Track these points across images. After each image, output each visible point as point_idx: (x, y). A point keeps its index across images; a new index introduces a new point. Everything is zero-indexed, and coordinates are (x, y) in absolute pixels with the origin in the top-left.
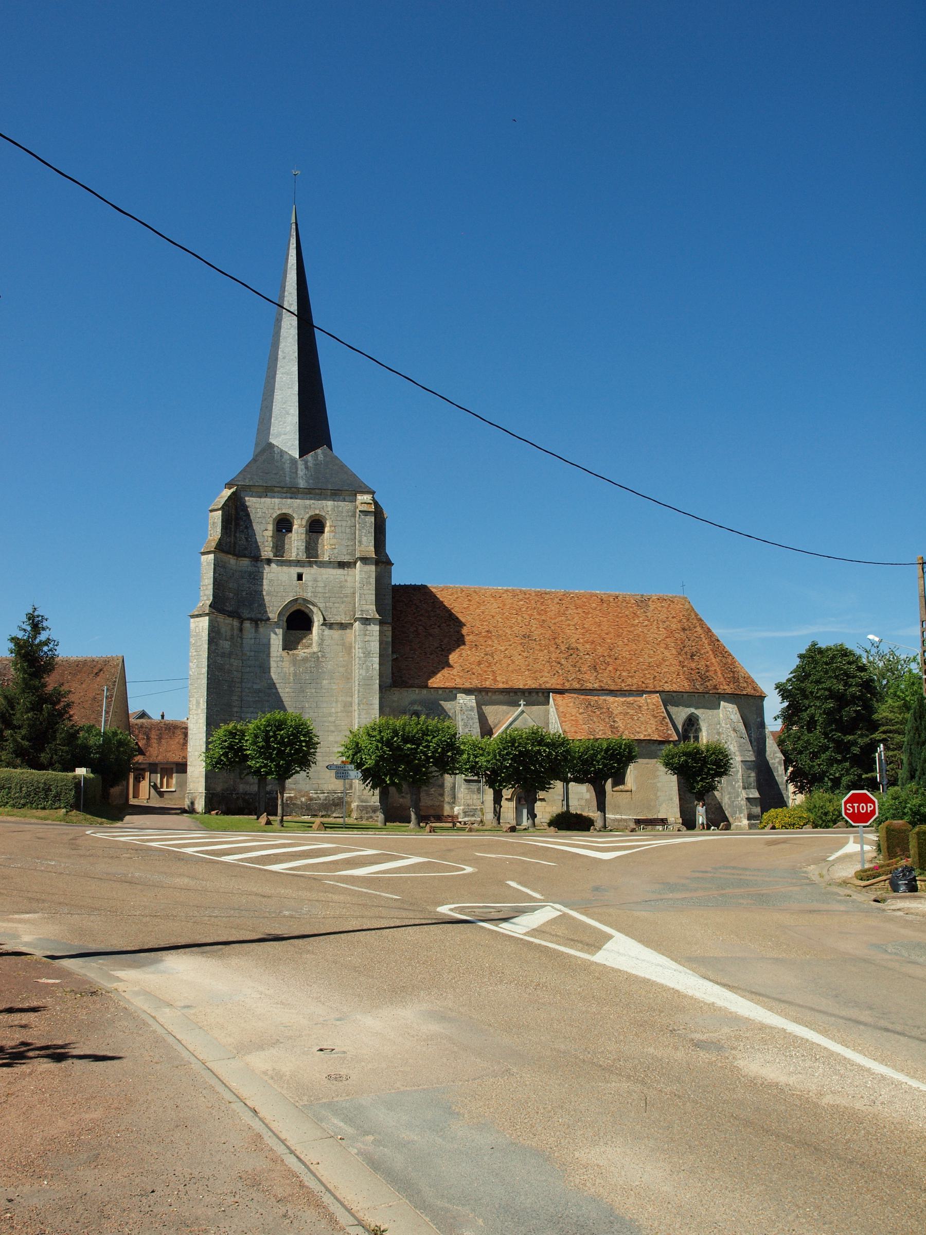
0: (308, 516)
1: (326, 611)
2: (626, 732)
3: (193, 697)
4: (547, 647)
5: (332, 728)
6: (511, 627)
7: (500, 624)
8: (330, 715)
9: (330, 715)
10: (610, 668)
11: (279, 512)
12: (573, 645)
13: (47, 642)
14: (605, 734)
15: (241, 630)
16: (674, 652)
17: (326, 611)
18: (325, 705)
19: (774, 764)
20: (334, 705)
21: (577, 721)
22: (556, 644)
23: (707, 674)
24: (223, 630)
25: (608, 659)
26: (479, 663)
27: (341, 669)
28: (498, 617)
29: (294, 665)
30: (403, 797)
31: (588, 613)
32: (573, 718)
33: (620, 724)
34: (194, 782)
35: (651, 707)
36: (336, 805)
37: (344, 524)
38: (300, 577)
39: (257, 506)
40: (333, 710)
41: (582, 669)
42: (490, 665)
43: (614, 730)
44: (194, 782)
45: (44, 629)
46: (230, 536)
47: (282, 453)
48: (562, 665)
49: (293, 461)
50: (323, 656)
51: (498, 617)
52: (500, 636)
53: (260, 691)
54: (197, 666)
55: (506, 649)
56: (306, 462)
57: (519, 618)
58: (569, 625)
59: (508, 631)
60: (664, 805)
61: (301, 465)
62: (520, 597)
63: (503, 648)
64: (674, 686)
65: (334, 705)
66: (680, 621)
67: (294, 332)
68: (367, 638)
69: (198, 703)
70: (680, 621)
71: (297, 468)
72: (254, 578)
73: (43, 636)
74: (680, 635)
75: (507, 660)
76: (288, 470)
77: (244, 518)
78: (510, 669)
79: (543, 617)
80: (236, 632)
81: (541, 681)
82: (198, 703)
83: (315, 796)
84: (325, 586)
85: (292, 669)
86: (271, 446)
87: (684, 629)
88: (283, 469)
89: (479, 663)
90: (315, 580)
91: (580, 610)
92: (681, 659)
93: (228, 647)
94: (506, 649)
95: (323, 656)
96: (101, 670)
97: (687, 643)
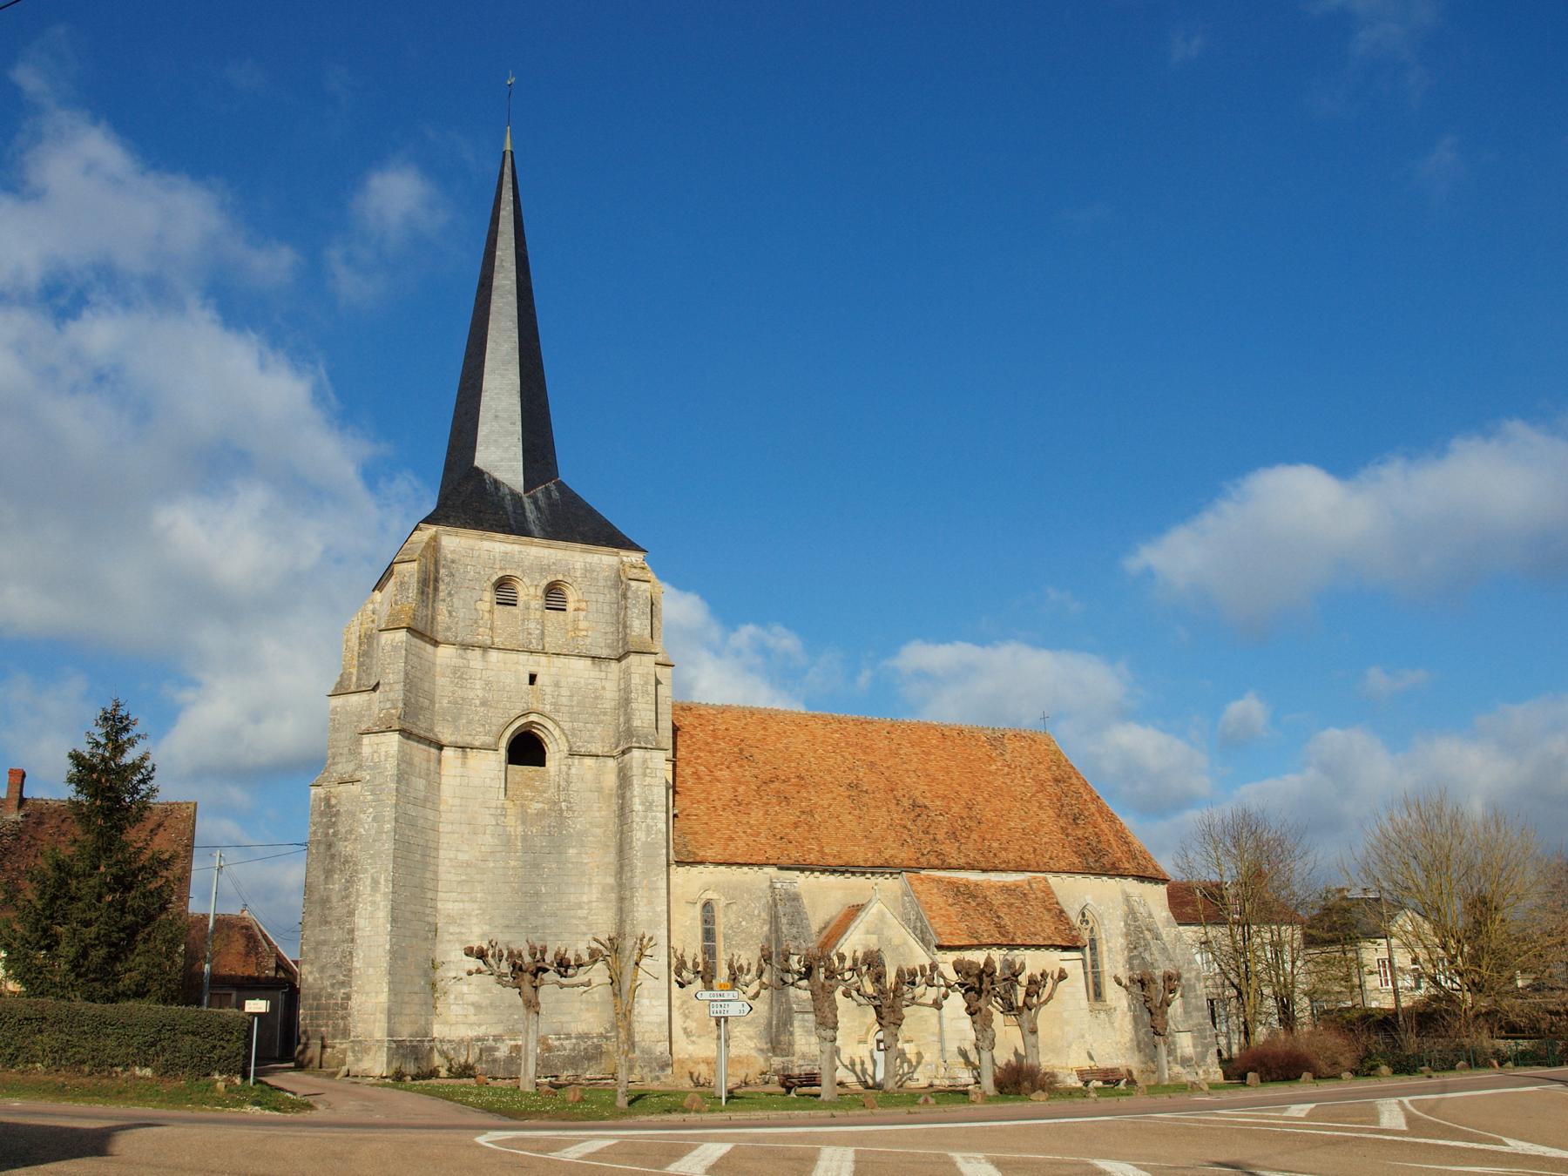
0: (545, 583)
1: (574, 735)
3: (366, 871)
5: (584, 929)
6: (830, 772)
8: (580, 906)
9: (580, 906)
10: (974, 836)
11: (501, 574)
12: (921, 801)
13: (135, 767)
15: (440, 761)
16: (1051, 812)
17: (574, 735)
19: (1188, 979)
20: (586, 889)
21: (949, 917)
24: (416, 760)
27: (598, 831)
28: (809, 755)
29: (524, 823)
31: (927, 754)
33: (1007, 921)
34: (365, 1022)
36: (590, 1059)
37: (601, 598)
38: (533, 679)
39: (468, 561)
40: (585, 898)
44: (365, 1022)
45: (131, 742)
47: (496, 481)
49: (513, 494)
50: (568, 809)
51: (809, 755)
52: (817, 784)
53: (468, 865)
54: (374, 819)
56: (535, 501)
61: (526, 500)
65: (586, 889)
67: (513, 299)
69: (375, 882)
70: (1049, 769)
71: (523, 508)
73: (130, 757)
75: (834, 821)
76: (510, 508)
77: (447, 579)
78: (841, 836)
79: (871, 758)
80: (433, 765)
81: (887, 854)
82: (375, 882)
84: (572, 696)
85: (520, 829)
86: (479, 473)
87: (1057, 781)
88: (504, 508)
89: (796, 825)
90: (557, 685)
91: (917, 750)
92: (1061, 823)
96: (160, 825)
97: (1066, 801)
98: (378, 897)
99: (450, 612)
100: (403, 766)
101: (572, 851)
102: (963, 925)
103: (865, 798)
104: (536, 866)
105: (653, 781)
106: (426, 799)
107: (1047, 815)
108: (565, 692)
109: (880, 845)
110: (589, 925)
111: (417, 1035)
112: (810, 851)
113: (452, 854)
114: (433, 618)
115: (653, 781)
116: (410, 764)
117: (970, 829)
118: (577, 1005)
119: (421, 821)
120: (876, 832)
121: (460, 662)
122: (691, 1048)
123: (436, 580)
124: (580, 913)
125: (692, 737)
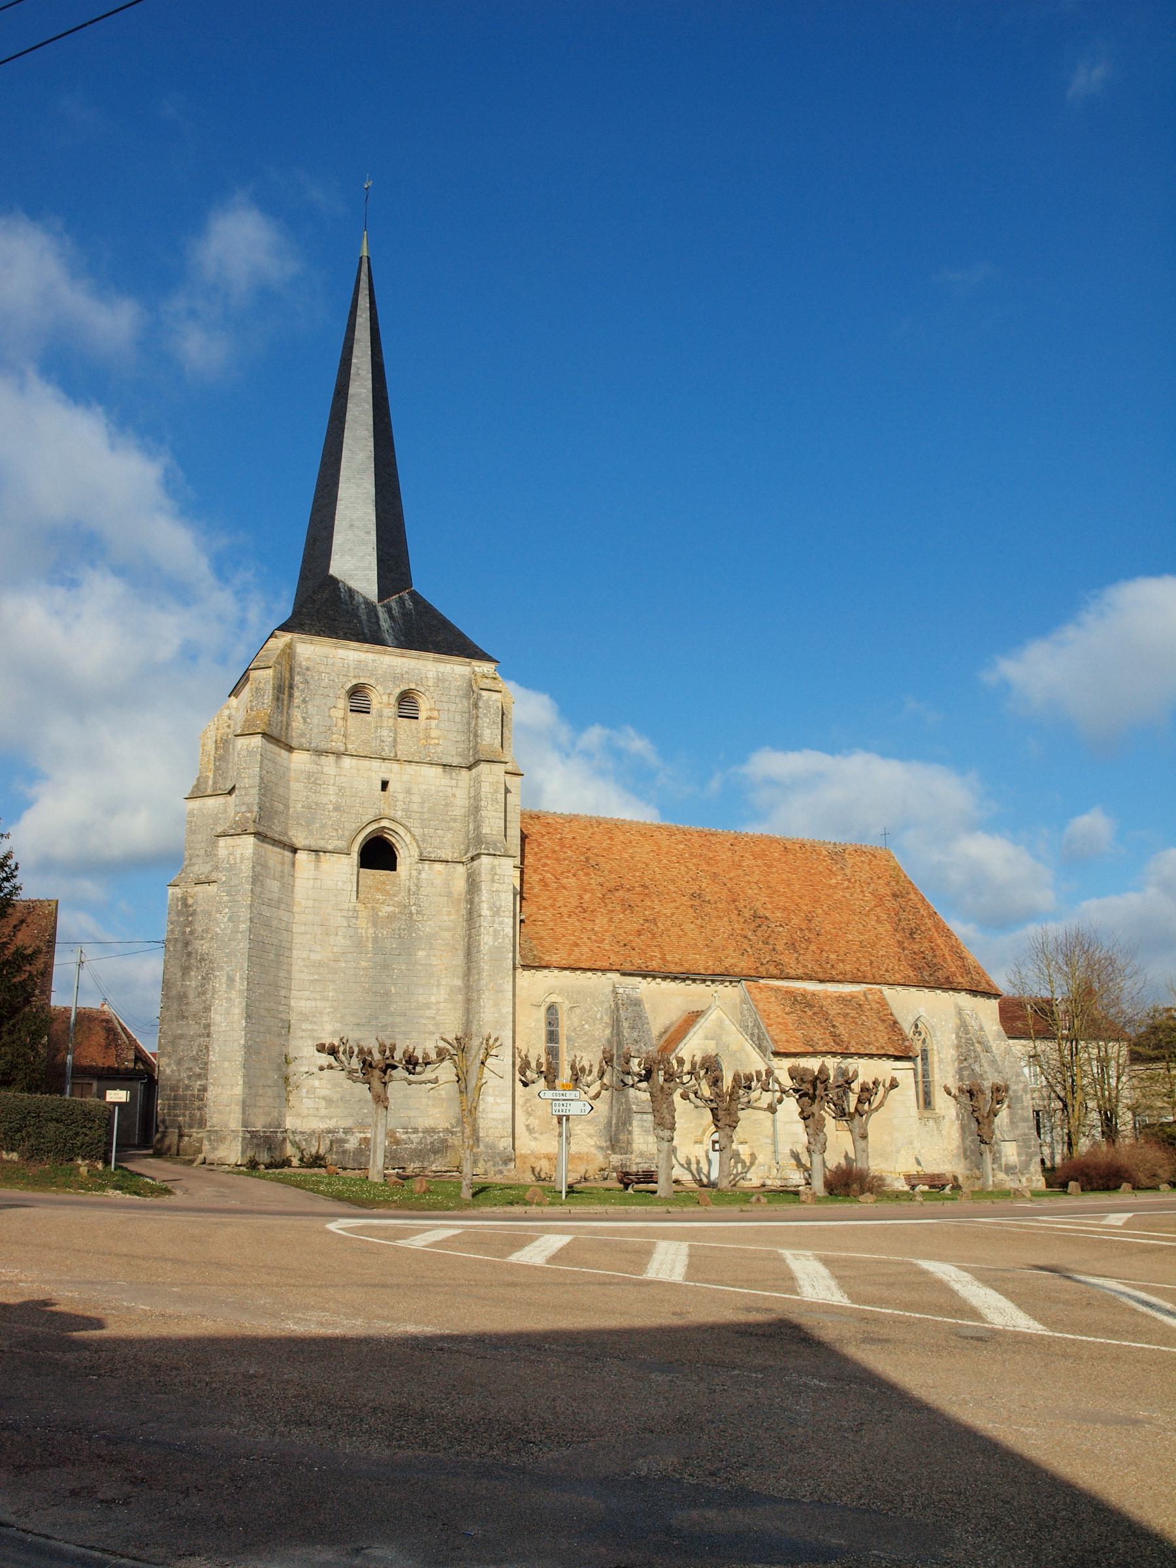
0: (398, 691)
2: (853, 1043)
3: (222, 969)
4: (729, 911)
5: (432, 1028)
6: (673, 882)
7: (658, 876)
8: (428, 1006)
9: (428, 1006)
10: (813, 947)
11: (354, 682)
12: (761, 912)
14: (826, 1044)
15: (293, 864)
18: (421, 991)
19: (1015, 1091)
20: (435, 990)
21: (785, 1024)
22: (737, 908)
23: (935, 961)
24: (271, 863)
25: (808, 935)
26: (639, 933)
27: (447, 935)
28: (654, 865)
29: (375, 925)
30: (535, 1138)
31: (770, 867)
32: (780, 1020)
33: (841, 1030)
35: (875, 1006)
36: (435, 1153)
37: (453, 707)
38: (385, 785)
39: (322, 668)
40: (433, 999)
41: (777, 947)
42: (654, 937)
43: (837, 1039)
44: (220, 1112)
46: (282, 712)
47: (351, 592)
48: (750, 940)
49: (368, 603)
50: (418, 913)
51: (654, 865)
52: (662, 893)
53: (321, 964)
54: (230, 919)
55: (673, 914)
56: (389, 610)
57: (683, 868)
58: (749, 883)
59: (672, 888)
60: (903, 1152)
61: (379, 609)
62: (679, 837)
63: (668, 912)
64: (898, 976)
65: (435, 990)
66: (888, 884)
67: (368, 407)
68: (496, 886)
69: (231, 980)
70: (888, 884)
71: (377, 617)
72: (314, 783)
74: (889, 903)
75: (676, 930)
76: (364, 617)
77: (301, 686)
80: (287, 868)
81: (728, 962)
82: (231, 980)
83: (404, 1137)
84: (423, 802)
85: (371, 931)
86: (334, 581)
87: (895, 895)
88: (358, 617)
89: (639, 933)
90: (408, 792)
91: (759, 862)
92: (898, 937)
93: (276, 890)
94: (673, 914)
95: (418, 913)
96: (22, 922)
97: (903, 916)
98: (234, 994)
99: (304, 719)
100: (258, 868)
101: (421, 954)
102: (799, 1033)
103: (708, 909)
104: (386, 967)
105: (501, 887)
106: (280, 901)
107: (884, 929)
108: (416, 798)
109: (720, 954)
110: (437, 1025)
111: (270, 1126)
112: (652, 958)
113: (305, 954)
114: (288, 725)
115: (501, 887)
116: (265, 866)
117: (809, 941)
118: (424, 1101)
119: (275, 923)
120: (717, 941)
121: (314, 768)
122: (533, 1144)
123: (291, 687)
124: (428, 1013)
125: (539, 845)
